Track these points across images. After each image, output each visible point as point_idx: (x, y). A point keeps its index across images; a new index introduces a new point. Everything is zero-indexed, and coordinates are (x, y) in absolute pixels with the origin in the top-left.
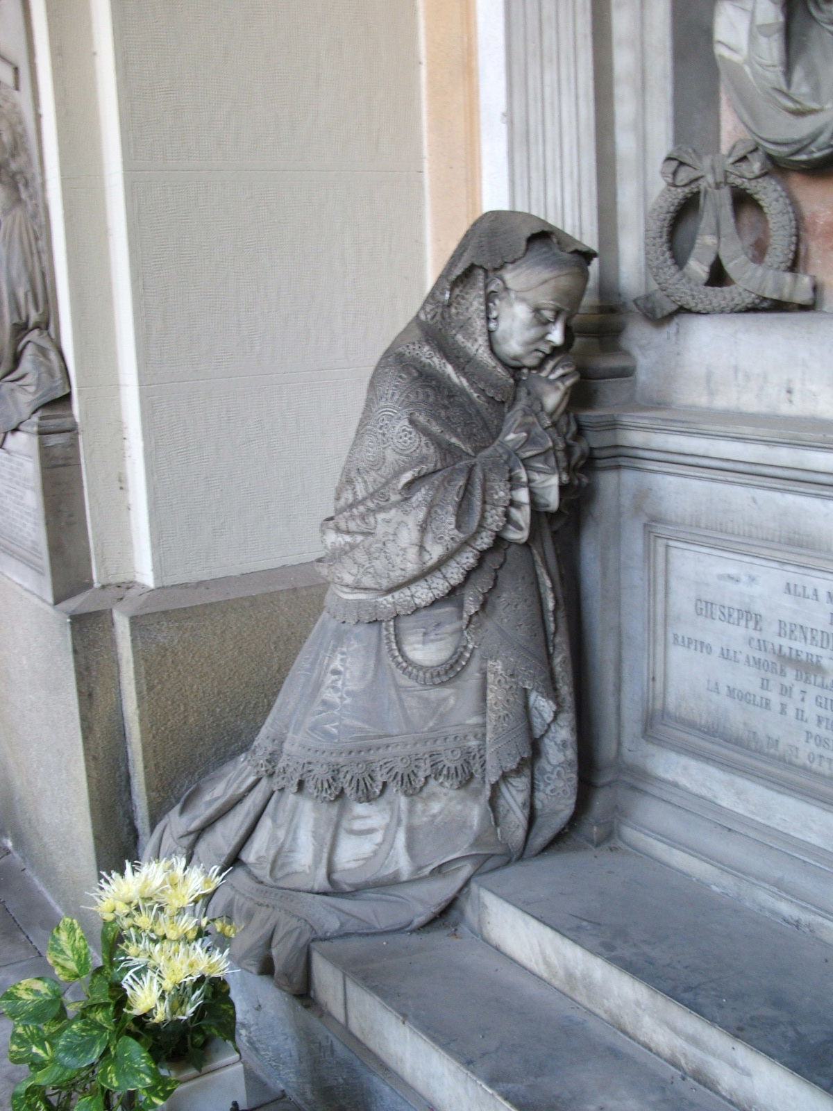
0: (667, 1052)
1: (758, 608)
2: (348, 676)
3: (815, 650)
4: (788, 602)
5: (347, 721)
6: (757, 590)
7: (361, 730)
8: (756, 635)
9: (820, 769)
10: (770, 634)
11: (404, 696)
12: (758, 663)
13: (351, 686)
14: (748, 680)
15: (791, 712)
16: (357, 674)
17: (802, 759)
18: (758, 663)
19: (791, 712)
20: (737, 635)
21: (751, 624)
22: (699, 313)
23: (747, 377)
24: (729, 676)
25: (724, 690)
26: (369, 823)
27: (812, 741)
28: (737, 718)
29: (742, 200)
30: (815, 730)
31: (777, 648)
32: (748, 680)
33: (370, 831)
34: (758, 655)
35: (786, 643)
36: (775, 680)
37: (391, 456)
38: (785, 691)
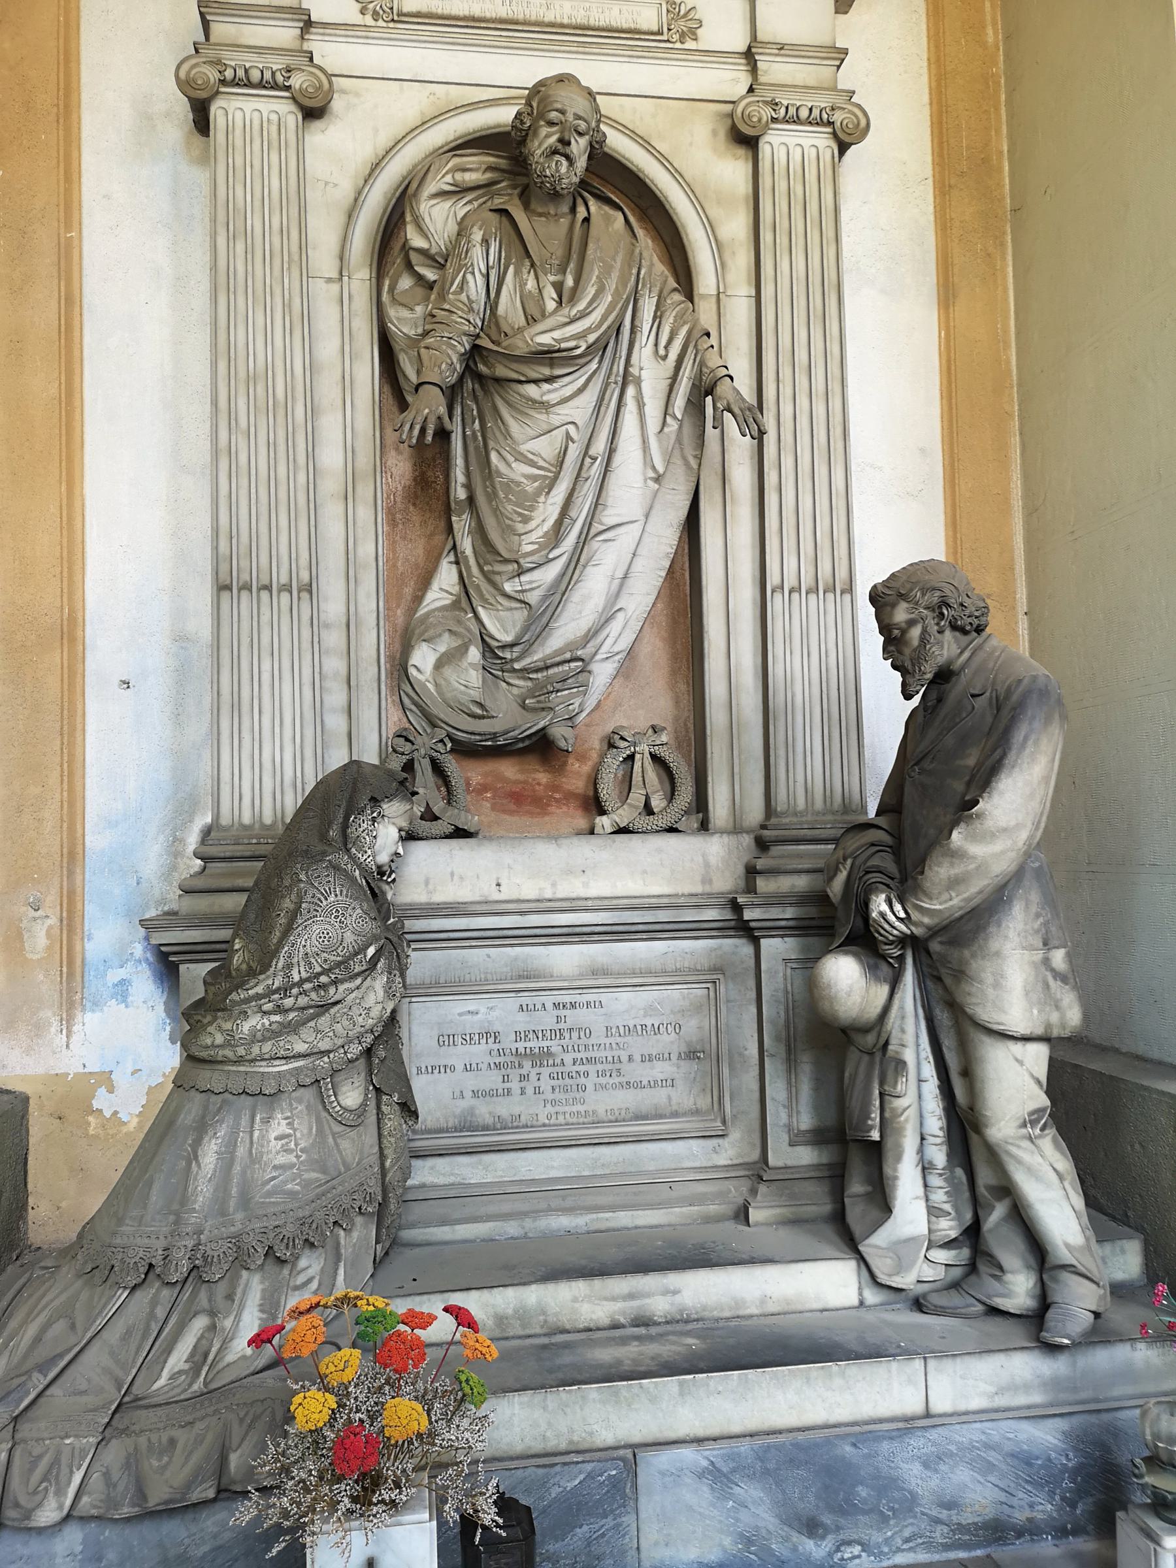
0: (606, 1321)
1: (497, 1027)
2: (298, 1135)
3: (545, 1044)
4: (522, 1017)
5: (306, 1176)
6: (495, 1014)
7: (317, 1180)
8: (496, 1046)
9: (558, 1122)
10: (508, 1042)
11: (339, 1141)
12: (498, 1066)
13: (303, 1144)
14: (493, 1080)
15: (530, 1091)
16: (305, 1131)
17: (543, 1119)
18: (498, 1066)
19: (530, 1091)
20: (479, 1052)
21: (491, 1040)
22: (421, 839)
23: (461, 878)
24: (471, 1082)
25: (468, 1094)
26: (310, 1272)
27: (548, 1105)
28: (484, 1111)
29: (437, 768)
30: (550, 1096)
31: (514, 1051)
32: (493, 1080)
33: (310, 1280)
34: (502, 1059)
35: (521, 1046)
36: (514, 1075)
37: (349, 937)
38: (523, 1078)
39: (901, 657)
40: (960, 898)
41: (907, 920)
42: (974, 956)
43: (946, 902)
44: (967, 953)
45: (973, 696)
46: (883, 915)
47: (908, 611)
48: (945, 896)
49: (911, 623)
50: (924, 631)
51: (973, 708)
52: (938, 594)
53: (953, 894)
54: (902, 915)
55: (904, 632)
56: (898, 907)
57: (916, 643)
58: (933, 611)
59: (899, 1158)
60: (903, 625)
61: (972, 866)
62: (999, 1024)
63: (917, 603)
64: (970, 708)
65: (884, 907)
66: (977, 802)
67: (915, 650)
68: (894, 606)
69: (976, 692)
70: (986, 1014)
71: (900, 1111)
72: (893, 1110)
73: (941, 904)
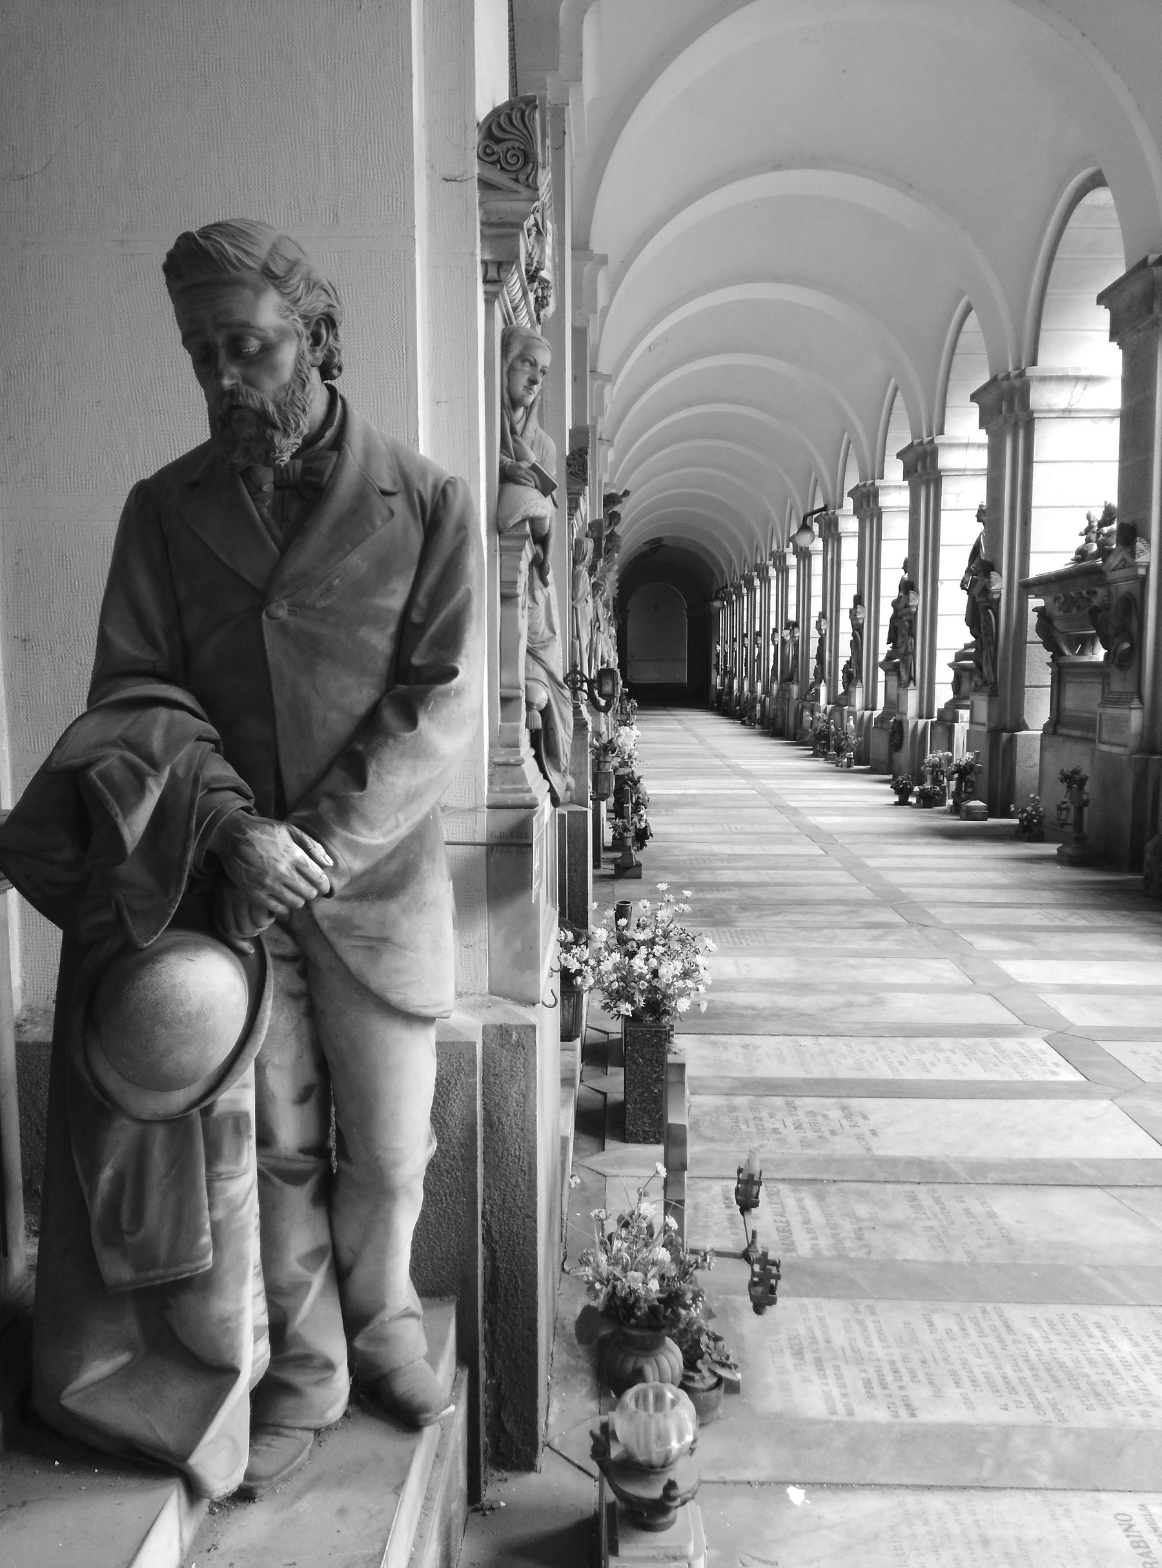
39: (256, 394)
40: (410, 823)
41: (334, 870)
42: (405, 911)
43: (391, 831)
44: (393, 907)
45: (385, 493)
46: (299, 869)
47: (283, 313)
48: (391, 823)
49: (283, 334)
50: (300, 358)
51: (392, 513)
52: (324, 297)
53: (401, 817)
54: (329, 862)
55: (268, 349)
56: (319, 850)
57: (287, 373)
58: (307, 325)
59: (241, 1281)
60: (271, 334)
61: (438, 772)
62: (437, 1005)
63: (296, 302)
64: (386, 513)
65: (299, 853)
66: (454, 673)
67: (286, 388)
68: (258, 292)
69: (387, 486)
70: (417, 999)
71: (240, 1199)
72: (229, 1202)
73: (384, 835)
